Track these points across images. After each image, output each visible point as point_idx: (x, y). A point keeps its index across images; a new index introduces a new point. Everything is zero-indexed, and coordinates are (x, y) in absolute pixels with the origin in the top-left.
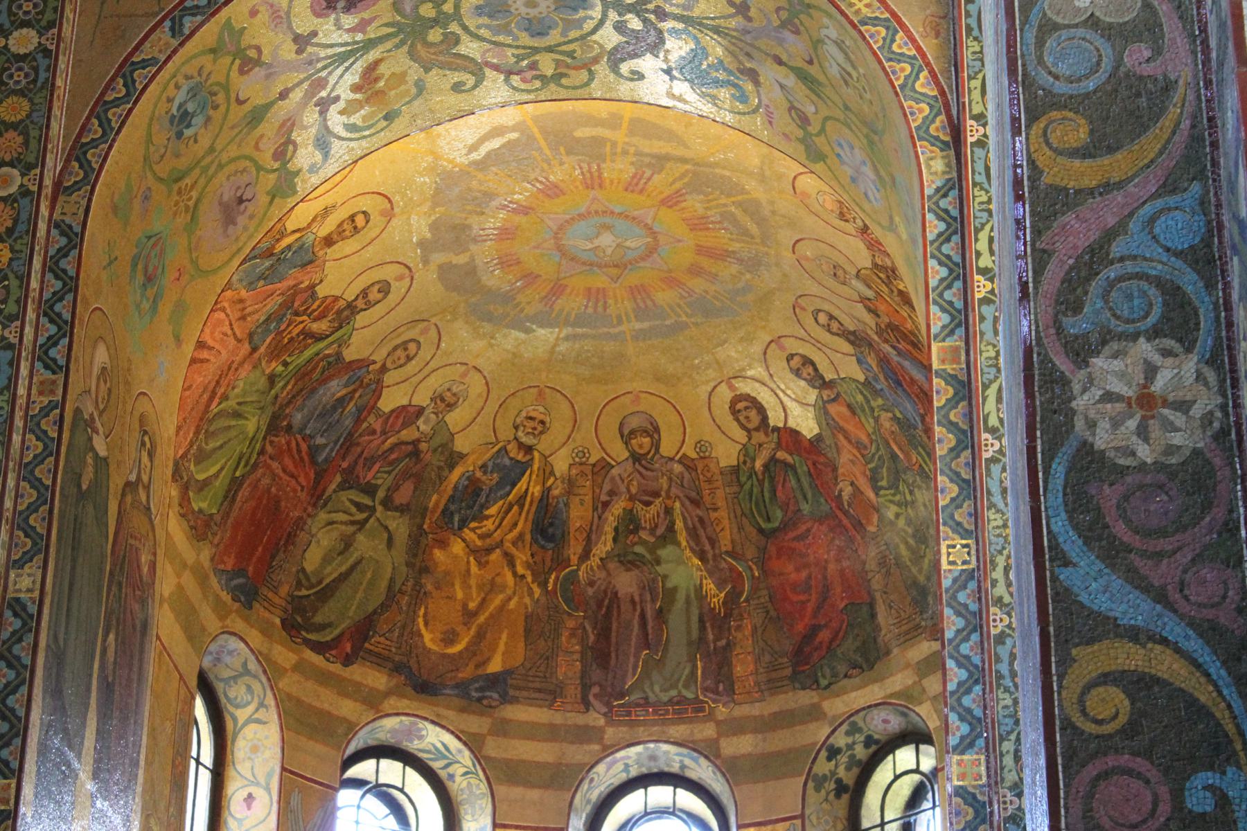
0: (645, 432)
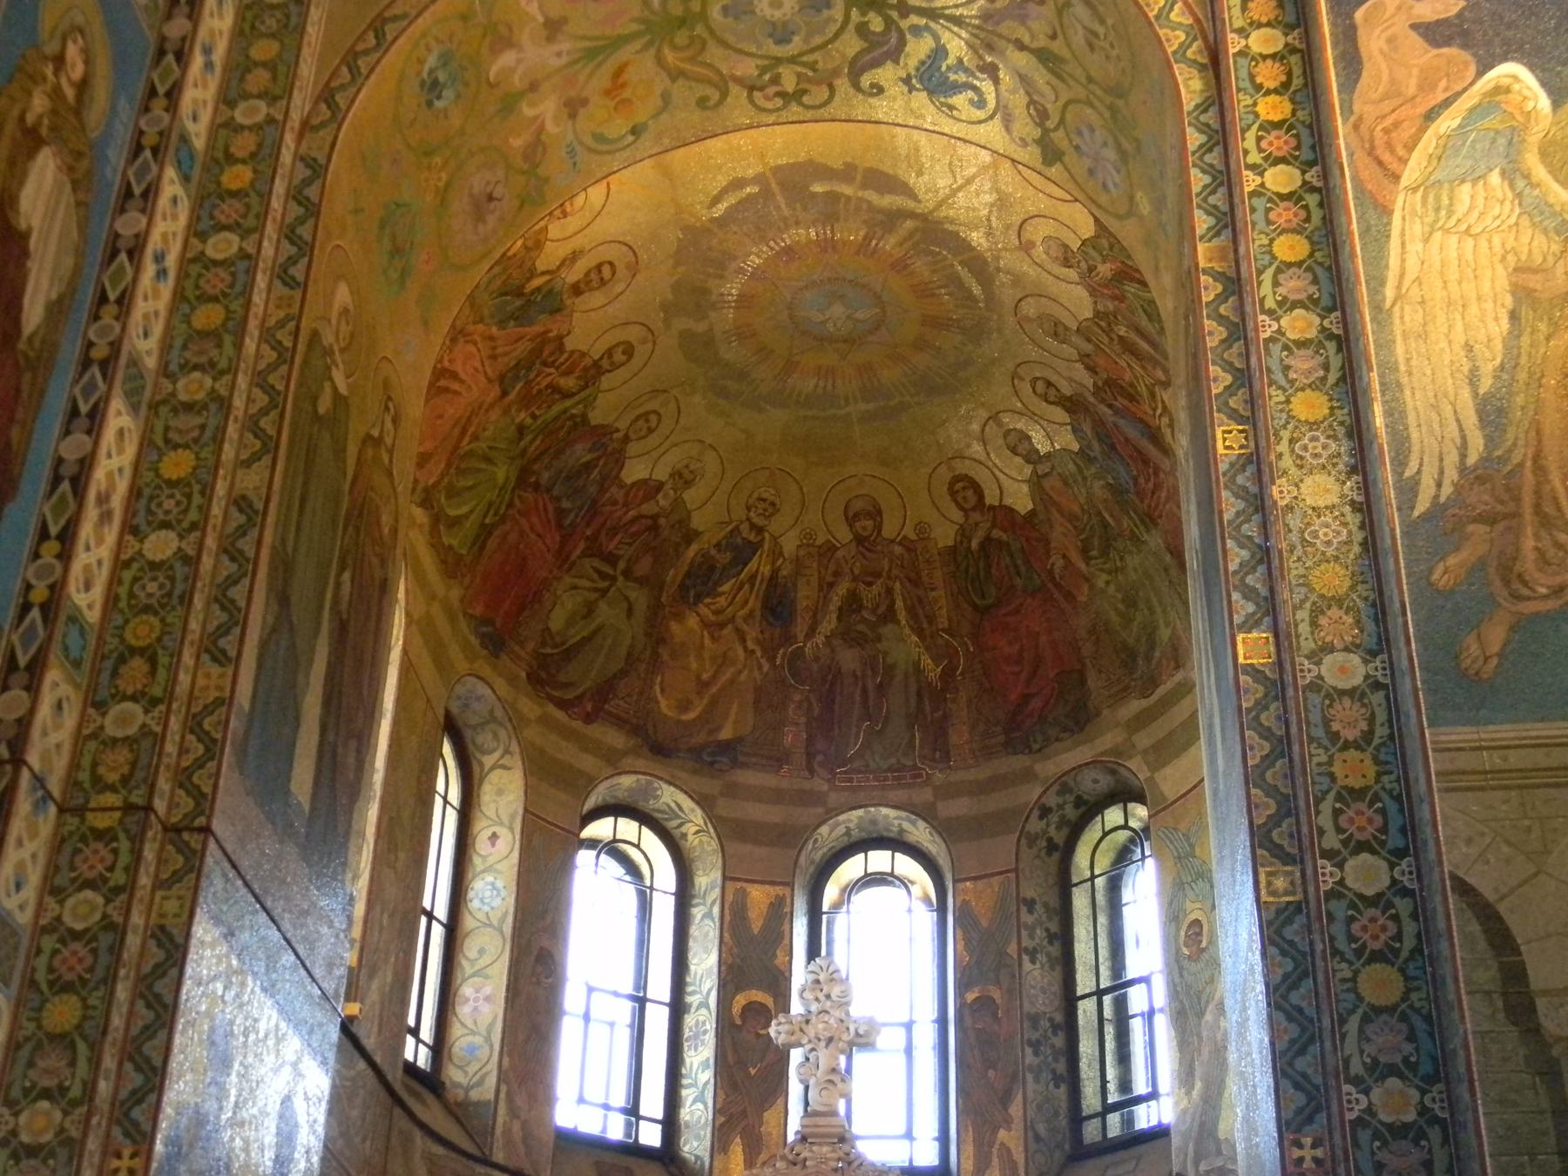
0: (869, 515)
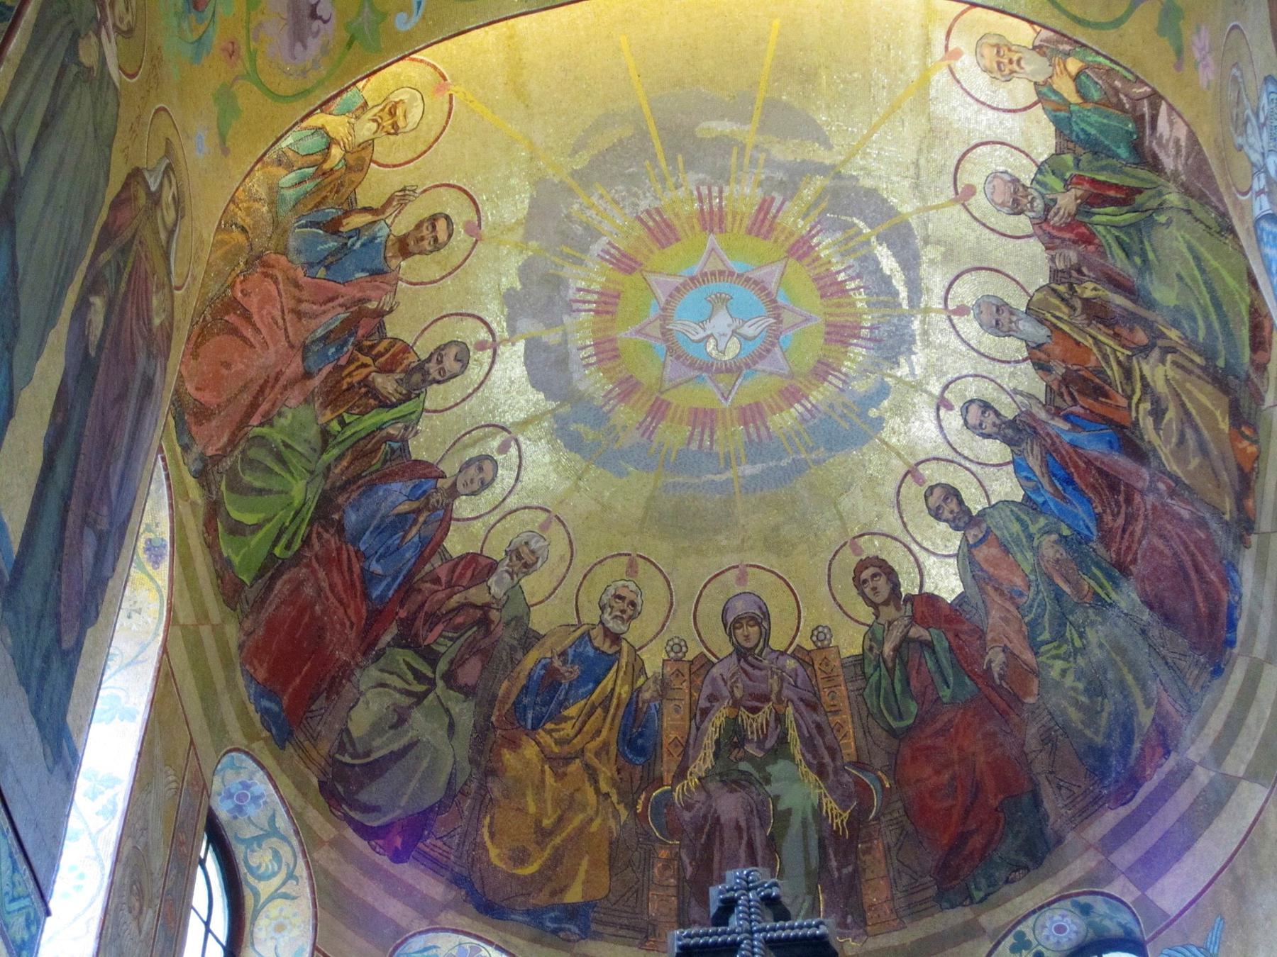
0: (753, 620)
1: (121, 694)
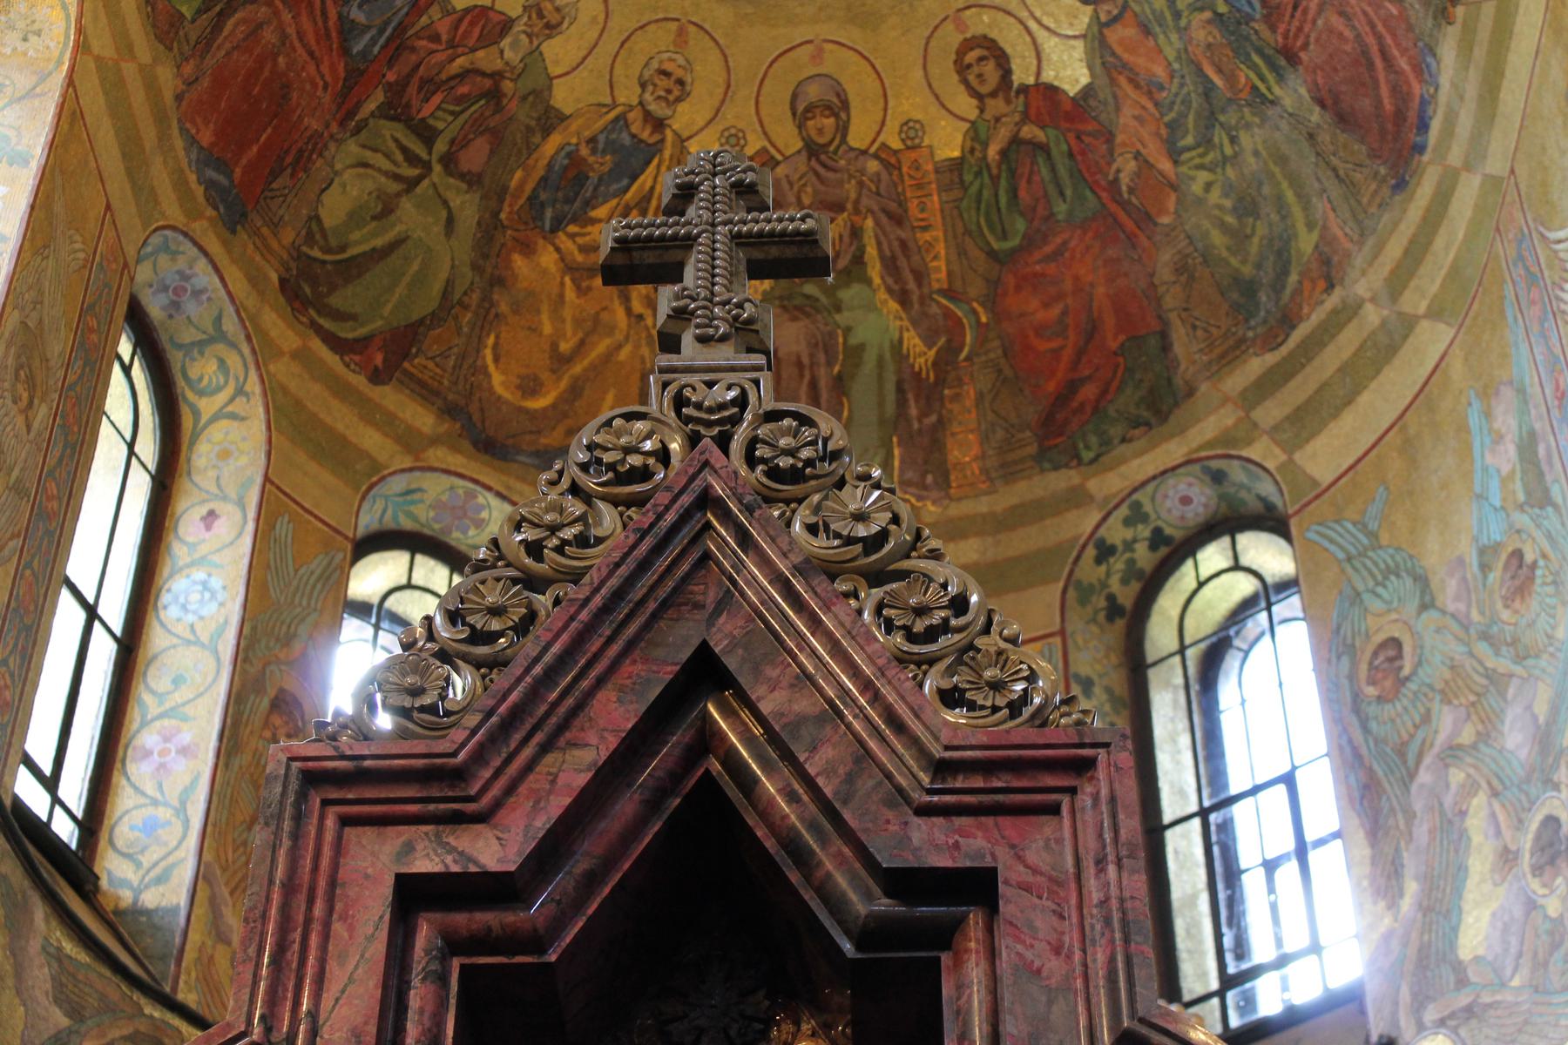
0: (829, 109)
1: (12, 134)
